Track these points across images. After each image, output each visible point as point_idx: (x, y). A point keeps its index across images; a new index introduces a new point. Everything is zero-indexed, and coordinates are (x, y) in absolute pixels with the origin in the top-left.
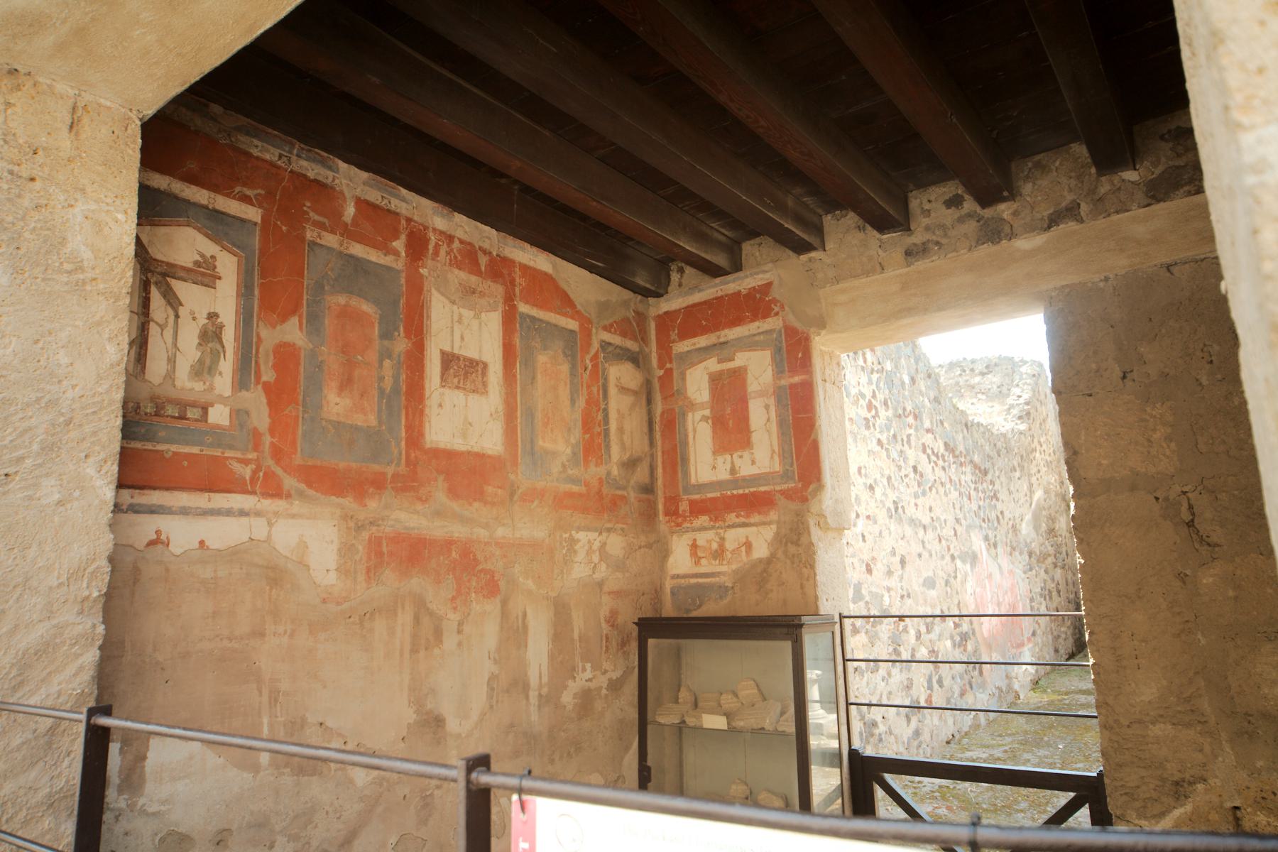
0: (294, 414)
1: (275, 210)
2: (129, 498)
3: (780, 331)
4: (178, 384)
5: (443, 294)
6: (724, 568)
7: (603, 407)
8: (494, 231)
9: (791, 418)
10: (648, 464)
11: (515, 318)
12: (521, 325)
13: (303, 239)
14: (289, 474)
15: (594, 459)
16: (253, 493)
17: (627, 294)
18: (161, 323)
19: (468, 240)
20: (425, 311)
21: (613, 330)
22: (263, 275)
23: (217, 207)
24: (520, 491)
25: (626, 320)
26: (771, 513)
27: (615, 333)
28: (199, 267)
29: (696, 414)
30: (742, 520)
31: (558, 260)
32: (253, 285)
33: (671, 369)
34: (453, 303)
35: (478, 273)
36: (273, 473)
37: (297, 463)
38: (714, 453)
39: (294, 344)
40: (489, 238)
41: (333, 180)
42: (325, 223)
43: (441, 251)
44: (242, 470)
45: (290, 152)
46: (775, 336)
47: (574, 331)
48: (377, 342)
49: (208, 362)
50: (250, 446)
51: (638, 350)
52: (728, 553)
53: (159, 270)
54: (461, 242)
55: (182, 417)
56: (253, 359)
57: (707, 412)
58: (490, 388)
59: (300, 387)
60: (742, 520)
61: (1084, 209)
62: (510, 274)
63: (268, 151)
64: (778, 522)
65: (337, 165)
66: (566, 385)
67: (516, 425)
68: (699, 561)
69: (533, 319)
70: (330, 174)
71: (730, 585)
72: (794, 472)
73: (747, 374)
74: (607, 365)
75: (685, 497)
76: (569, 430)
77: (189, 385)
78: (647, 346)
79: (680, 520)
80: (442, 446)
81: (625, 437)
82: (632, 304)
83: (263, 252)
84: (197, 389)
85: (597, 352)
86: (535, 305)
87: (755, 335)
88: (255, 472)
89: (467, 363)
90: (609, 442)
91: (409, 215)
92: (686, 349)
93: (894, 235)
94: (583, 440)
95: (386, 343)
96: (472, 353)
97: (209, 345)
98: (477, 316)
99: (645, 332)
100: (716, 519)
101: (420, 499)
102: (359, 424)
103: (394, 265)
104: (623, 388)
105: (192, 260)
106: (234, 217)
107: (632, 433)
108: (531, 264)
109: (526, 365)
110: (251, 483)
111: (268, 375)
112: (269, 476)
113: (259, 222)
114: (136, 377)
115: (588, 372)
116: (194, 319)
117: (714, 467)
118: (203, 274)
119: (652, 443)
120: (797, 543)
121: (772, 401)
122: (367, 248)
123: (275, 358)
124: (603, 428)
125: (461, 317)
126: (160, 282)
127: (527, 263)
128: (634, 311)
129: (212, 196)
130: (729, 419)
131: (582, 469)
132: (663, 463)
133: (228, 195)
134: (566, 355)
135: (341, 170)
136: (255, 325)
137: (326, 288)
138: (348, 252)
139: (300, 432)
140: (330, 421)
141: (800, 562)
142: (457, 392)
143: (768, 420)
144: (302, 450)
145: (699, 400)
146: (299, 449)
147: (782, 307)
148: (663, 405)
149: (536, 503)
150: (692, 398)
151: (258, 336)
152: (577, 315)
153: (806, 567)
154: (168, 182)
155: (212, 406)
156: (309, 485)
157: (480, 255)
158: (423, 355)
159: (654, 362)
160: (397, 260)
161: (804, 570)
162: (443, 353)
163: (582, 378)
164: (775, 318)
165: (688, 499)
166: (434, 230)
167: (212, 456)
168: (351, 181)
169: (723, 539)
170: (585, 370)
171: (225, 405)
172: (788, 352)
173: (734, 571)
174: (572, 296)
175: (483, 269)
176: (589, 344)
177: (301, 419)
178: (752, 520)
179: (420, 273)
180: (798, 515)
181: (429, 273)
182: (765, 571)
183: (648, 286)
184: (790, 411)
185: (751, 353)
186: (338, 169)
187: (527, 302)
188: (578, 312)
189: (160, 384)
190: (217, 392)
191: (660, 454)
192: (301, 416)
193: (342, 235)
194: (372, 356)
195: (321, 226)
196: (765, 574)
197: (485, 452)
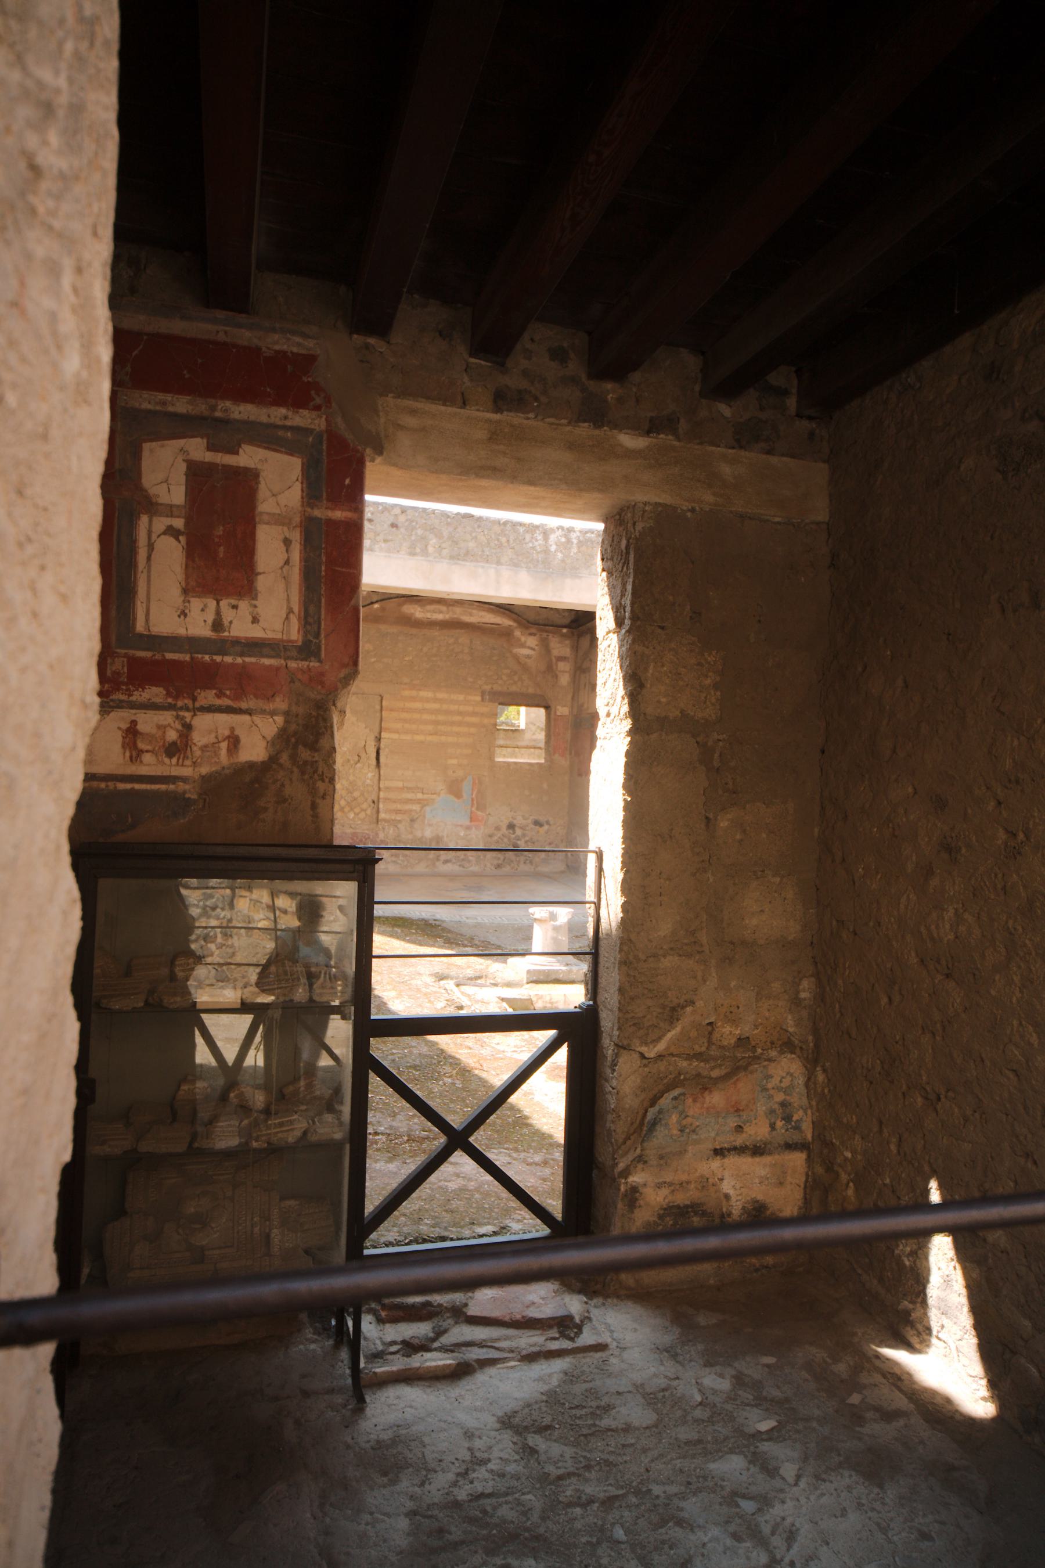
6: (186, 771)
9: (323, 568)
26: (277, 699)
29: (155, 519)
38: (185, 591)
46: (311, 439)
52: (195, 748)
57: (179, 523)
60: (226, 702)
61: (683, 425)
64: (287, 714)
68: (138, 756)
71: (194, 796)
72: (319, 648)
73: (258, 483)
87: (277, 427)
92: (145, 406)
93: (483, 363)
117: (184, 614)
120: (313, 747)
121: (296, 536)
141: (315, 772)
143: (287, 562)
145: (164, 498)
147: (328, 400)
150: (152, 491)
153: (323, 781)
161: (319, 784)
164: (315, 414)
165: (126, 655)
169: (188, 727)
173: (203, 777)
178: (244, 705)
184: (324, 559)
196: (257, 785)
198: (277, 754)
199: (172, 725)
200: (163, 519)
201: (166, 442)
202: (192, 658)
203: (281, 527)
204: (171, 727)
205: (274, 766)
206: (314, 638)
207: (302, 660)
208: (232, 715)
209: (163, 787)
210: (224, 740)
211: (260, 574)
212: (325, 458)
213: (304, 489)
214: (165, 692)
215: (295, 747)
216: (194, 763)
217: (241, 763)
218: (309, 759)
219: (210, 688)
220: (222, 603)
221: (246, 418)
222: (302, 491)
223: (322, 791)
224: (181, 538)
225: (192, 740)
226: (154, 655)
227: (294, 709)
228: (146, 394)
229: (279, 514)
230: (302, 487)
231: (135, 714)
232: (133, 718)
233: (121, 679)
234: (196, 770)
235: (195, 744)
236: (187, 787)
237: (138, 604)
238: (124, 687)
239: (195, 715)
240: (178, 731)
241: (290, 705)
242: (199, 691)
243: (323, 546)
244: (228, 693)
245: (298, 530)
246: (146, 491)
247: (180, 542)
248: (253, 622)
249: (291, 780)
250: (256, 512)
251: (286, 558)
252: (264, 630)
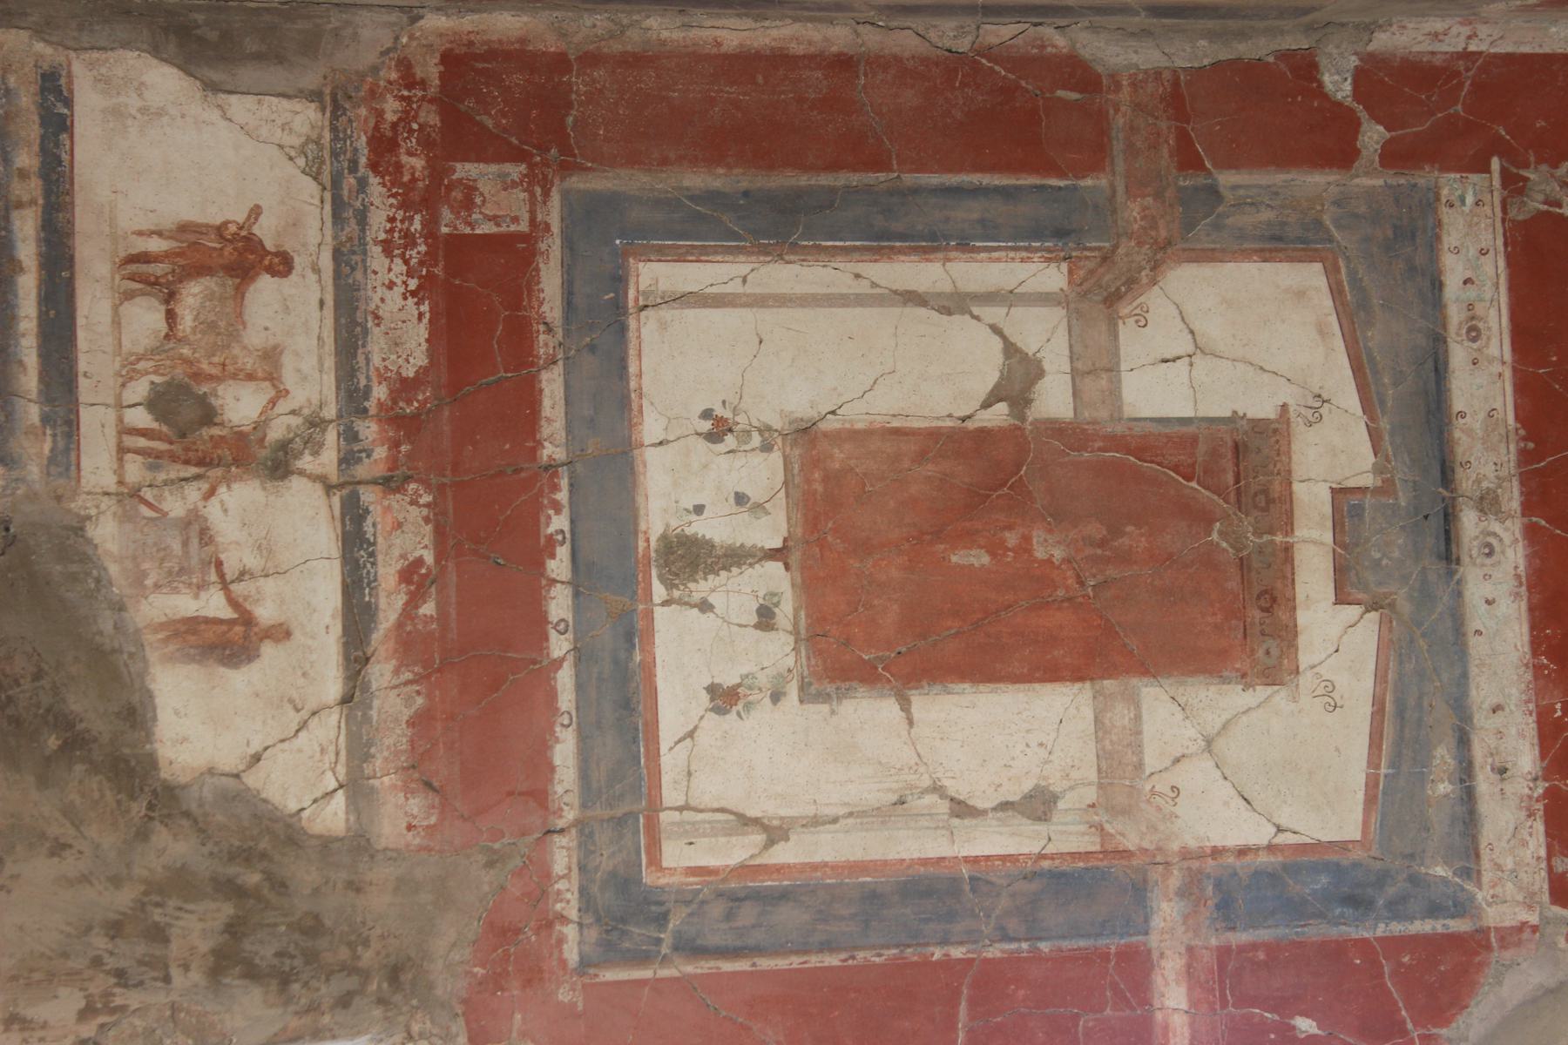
3: (1462, 906)
9: (957, 952)
26: (416, 805)
29: (1057, 314)
30: (390, 604)
38: (805, 433)
46: (1440, 871)
52: (193, 493)
60: (390, 604)
64: (359, 844)
68: (152, 283)
72: (643, 959)
75: (553, 215)
79: (416, 164)
87: (1464, 741)
92: (1454, 270)
100: (402, 425)
117: (719, 429)
130: (995, 549)
132: (779, 60)
143: (962, 809)
150: (1155, 300)
153: (86, 1013)
161: (69, 1002)
165: (538, 228)
169: (279, 466)
172: (1336, 951)
173: (79, 530)
178: (381, 673)
180: (394, 974)
182: (76, 742)
184: (995, 952)
185: (1362, 712)
196: (53, 742)
198: (187, 814)
199: (283, 406)
200: (1061, 342)
201: (1339, 344)
202: (552, 468)
203: (1093, 775)
204: (273, 402)
205: (138, 808)
206: (678, 934)
207: (583, 891)
208: (337, 628)
209: (30, 380)
210: (233, 603)
211: (905, 705)
212: (1381, 930)
213: (1249, 858)
214: (410, 373)
215: (230, 889)
216: (135, 493)
217: (143, 674)
218: (175, 949)
219: (440, 534)
220: (776, 567)
221: (1474, 624)
222: (1242, 852)
223: (39, 1011)
224: (1002, 408)
225: (228, 481)
226: (549, 330)
227: (383, 873)
228: (1494, 269)
229: (1139, 766)
230: (1256, 849)
231: (317, 270)
232: (298, 261)
233: (446, 214)
234: (106, 503)
235: (211, 493)
236: (34, 471)
237: (740, 267)
238: (417, 225)
239: (329, 488)
240: (261, 425)
241: (394, 855)
242: (426, 498)
243: (1045, 947)
244: (428, 609)
245: (1090, 843)
246: (1154, 282)
247: (986, 405)
248: (713, 690)
249: (85, 879)
250: (1135, 681)
251: (980, 804)
252: (691, 734)
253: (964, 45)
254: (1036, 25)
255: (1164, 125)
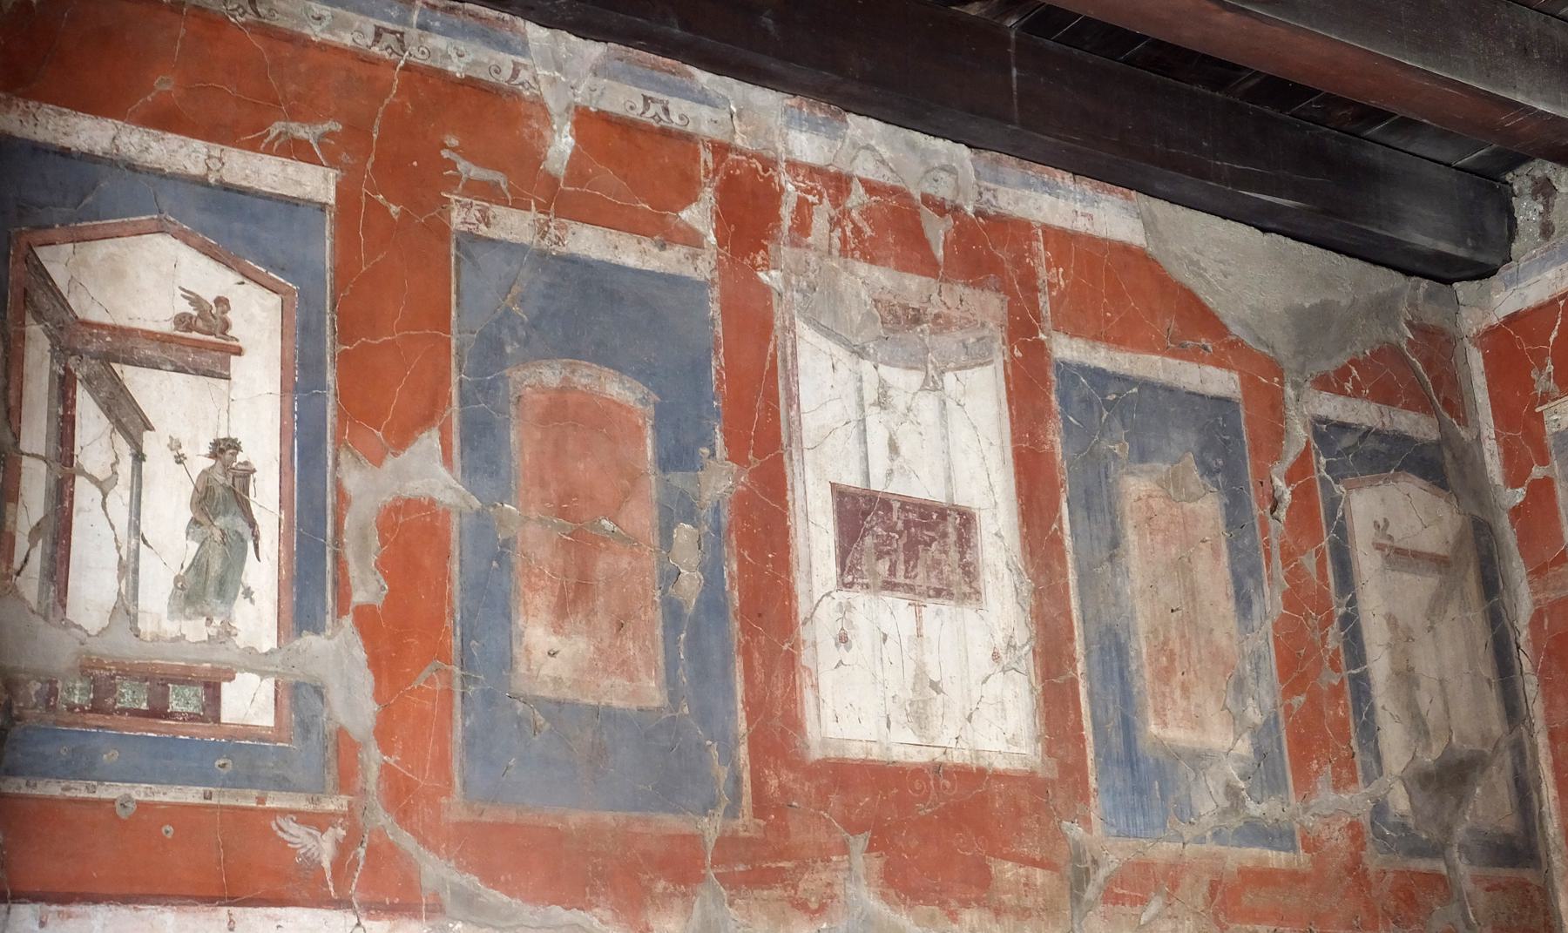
0: (438, 687)
1: (369, 166)
2: (36, 928)
4: (146, 626)
5: (828, 333)
7: (1341, 611)
8: (963, 151)
10: (1508, 773)
11: (1045, 380)
12: (1064, 400)
13: (443, 231)
14: (437, 852)
15: (1328, 768)
16: (342, 903)
17: (1382, 280)
18: (101, 477)
19: (891, 183)
20: (781, 383)
21: (1349, 386)
22: (345, 333)
23: (227, 179)
24: (1102, 873)
25: (1388, 353)
27: (1357, 393)
28: (189, 329)
31: (1160, 208)
32: (321, 361)
33: (1547, 483)
34: (860, 353)
35: (926, 265)
36: (391, 846)
37: (454, 817)
39: (432, 502)
40: (951, 171)
41: (515, 74)
42: (498, 184)
43: (815, 217)
44: (310, 843)
45: (405, 22)
47: (1227, 400)
48: (653, 478)
49: (216, 567)
50: (330, 779)
51: (1434, 436)
53: (92, 348)
54: (871, 188)
55: (158, 712)
56: (328, 549)
58: (987, 579)
59: (452, 614)
62: (1018, 261)
63: (346, 26)
65: (524, 34)
66: (1216, 553)
67: (1074, 682)
69: (1099, 377)
70: (506, 60)
74: (1340, 489)
76: (1240, 685)
77: (171, 627)
78: (1464, 422)
80: (855, 752)
81: (1424, 699)
82: (1403, 308)
83: (343, 273)
84: (191, 636)
85: (1305, 455)
86: (1099, 337)
88: (343, 848)
89: (911, 516)
90: (1372, 711)
91: (719, 135)
94: (1287, 715)
95: (677, 479)
96: (924, 486)
97: (220, 522)
98: (932, 385)
99: (1454, 383)
101: (802, 906)
102: (616, 703)
103: (687, 271)
104: (1399, 552)
105: (171, 314)
106: (269, 197)
107: (1441, 682)
108: (1081, 225)
109: (1088, 509)
110: (335, 876)
111: (368, 589)
112: (383, 856)
113: (332, 202)
114: (46, 618)
115: (1282, 514)
116: (180, 459)
118: (199, 346)
119: (1513, 710)
122: (613, 236)
123: (384, 542)
124: (1345, 673)
125: (884, 389)
126: (98, 377)
127: (1067, 225)
128: (1410, 324)
129: (216, 153)
131: (1293, 801)
133: (253, 147)
134: (1208, 471)
135: (533, 45)
136: (330, 462)
137: (509, 350)
138: (564, 250)
139: (458, 734)
140: (537, 701)
142: (888, 598)
144: (464, 784)
146: (457, 781)
148: (1535, 593)
149: (1154, 906)
151: (338, 485)
152: (1228, 351)
154: (112, 133)
155: (231, 679)
156: (490, 877)
157: (928, 216)
158: (785, 506)
159: (1494, 468)
160: (695, 257)
162: (841, 495)
163: (1264, 533)
166: (793, 166)
167: (235, 808)
168: (559, 69)
170: (1272, 512)
171: (263, 674)
174: (1210, 301)
175: (940, 253)
176: (1279, 434)
177: (458, 699)
179: (759, 282)
181: (787, 282)
183: (1445, 247)
186: (526, 44)
187: (1075, 332)
188: (1236, 345)
189: (100, 633)
190: (241, 641)
191: (1542, 740)
192: (458, 690)
193: (543, 209)
194: (641, 517)
195: (488, 192)
197: (983, 763)
253: (1534, 679)
254: (1518, 648)
255: (1550, 574)
